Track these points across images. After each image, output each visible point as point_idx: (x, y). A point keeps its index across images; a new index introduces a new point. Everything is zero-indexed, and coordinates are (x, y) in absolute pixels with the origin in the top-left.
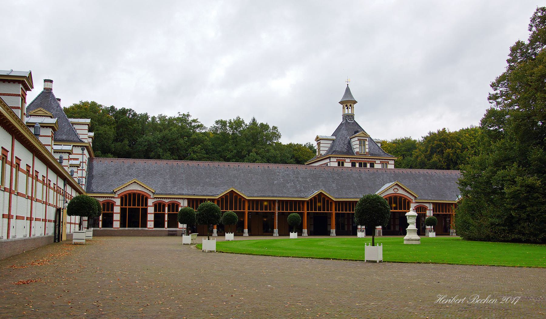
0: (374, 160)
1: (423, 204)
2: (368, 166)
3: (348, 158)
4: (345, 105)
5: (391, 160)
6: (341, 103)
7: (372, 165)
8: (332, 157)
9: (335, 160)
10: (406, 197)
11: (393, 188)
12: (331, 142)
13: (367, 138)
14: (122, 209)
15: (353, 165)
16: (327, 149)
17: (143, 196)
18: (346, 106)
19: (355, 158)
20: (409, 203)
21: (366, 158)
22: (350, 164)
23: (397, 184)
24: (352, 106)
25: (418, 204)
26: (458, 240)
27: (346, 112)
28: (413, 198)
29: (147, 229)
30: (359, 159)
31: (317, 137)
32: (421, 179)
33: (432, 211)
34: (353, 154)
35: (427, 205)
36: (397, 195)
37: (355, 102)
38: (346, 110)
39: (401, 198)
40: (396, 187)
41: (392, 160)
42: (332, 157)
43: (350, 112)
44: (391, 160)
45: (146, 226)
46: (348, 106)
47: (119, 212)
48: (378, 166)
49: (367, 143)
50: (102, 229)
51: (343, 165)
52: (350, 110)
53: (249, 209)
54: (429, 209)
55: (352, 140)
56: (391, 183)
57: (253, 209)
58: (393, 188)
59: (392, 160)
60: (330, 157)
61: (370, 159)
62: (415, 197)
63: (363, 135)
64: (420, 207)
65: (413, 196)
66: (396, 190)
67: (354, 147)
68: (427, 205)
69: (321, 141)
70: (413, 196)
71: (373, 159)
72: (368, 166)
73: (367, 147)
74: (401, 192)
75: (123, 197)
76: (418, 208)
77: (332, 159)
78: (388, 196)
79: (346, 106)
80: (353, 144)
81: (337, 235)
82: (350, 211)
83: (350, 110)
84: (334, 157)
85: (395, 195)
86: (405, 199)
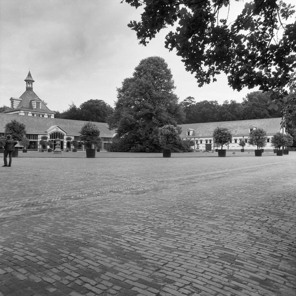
2: (41, 116)
6: (26, 81)
7: (43, 116)
9: (23, 111)
11: (56, 128)
12: (20, 102)
13: (41, 102)
15: (33, 115)
16: (17, 105)
18: (29, 83)
20: (63, 136)
22: (31, 114)
23: (58, 126)
26: (106, 152)
28: (65, 133)
31: (11, 98)
32: (69, 124)
34: (33, 109)
35: (72, 137)
37: (33, 81)
38: (28, 85)
39: (59, 133)
40: (57, 128)
46: (30, 82)
49: (40, 104)
55: (32, 102)
56: (55, 126)
58: (56, 128)
60: (20, 110)
62: (66, 133)
63: (38, 100)
65: (65, 132)
66: (57, 129)
67: (33, 105)
68: (72, 137)
69: (14, 101)
70: (65, 132)
72: (41, 116)
73: (40, 106)
74: (60, 130)
77: (21, 111)
78: (54, 132)
79: (29, 83)
80: (33, 104)
86: (62, 134)
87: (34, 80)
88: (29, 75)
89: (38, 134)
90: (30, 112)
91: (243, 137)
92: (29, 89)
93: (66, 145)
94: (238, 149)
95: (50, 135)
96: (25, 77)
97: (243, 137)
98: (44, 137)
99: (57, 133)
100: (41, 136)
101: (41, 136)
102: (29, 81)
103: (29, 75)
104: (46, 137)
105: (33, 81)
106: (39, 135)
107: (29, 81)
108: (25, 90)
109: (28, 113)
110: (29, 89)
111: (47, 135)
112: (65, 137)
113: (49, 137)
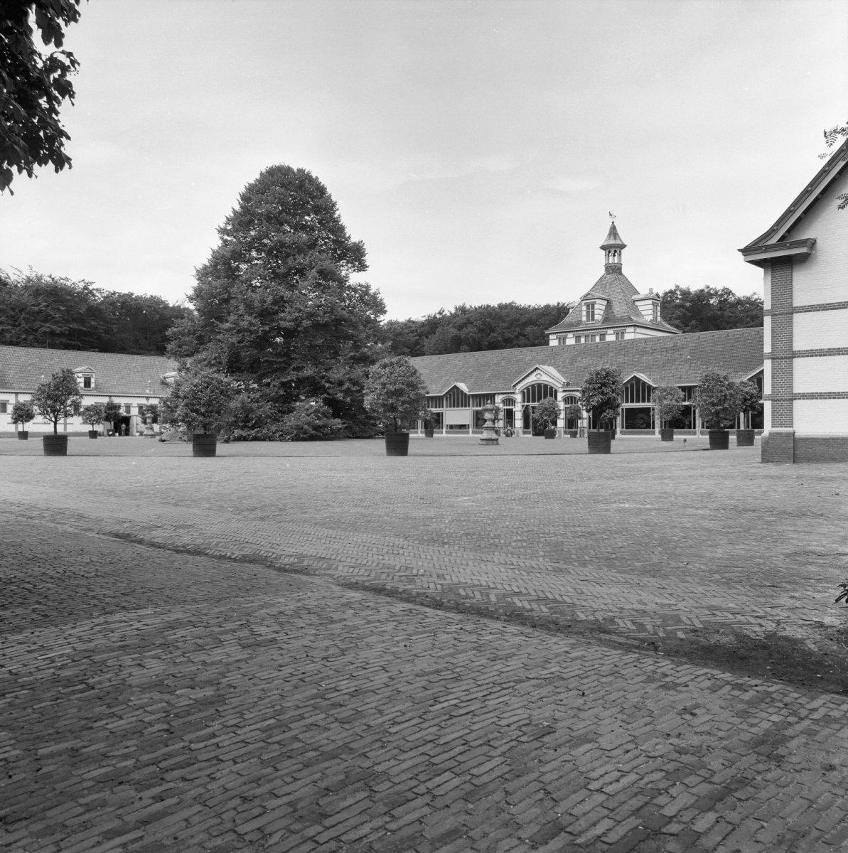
1: (573, 393)
5: (629, 326)
8: (551, 333)
11: (535, 373)
15: (578, 338)
20: (556, 391)
24: (618, 252)
25: (566, 393)
36: (539, 382)
39: (546, 386)
42: (551, 333)
44: (629, 326)
48: (611, 337)
52: (616, 258)
66: (538, 376)
84: (553, 333)
85: (537, 382)
87: (626, 244)
88: (613, 232)
89: (494, 395)
91: (17, 397)
92: (614, 270)
93: (520, 417)
94: (82, 431)
95: (523, 393)
96: (603, 239)
97: (17, 397)
98: (506, 400)
99: (539, 385)
102: (614, 248)
103: (613, 232)
104: (572, 397)
105: (623, 246)
106: (496, 397)
107: (614, 248)
108: (602, 271)
110: (614, 270)
111: (513, 393)
112: (560, 396)
113: (518, 397)
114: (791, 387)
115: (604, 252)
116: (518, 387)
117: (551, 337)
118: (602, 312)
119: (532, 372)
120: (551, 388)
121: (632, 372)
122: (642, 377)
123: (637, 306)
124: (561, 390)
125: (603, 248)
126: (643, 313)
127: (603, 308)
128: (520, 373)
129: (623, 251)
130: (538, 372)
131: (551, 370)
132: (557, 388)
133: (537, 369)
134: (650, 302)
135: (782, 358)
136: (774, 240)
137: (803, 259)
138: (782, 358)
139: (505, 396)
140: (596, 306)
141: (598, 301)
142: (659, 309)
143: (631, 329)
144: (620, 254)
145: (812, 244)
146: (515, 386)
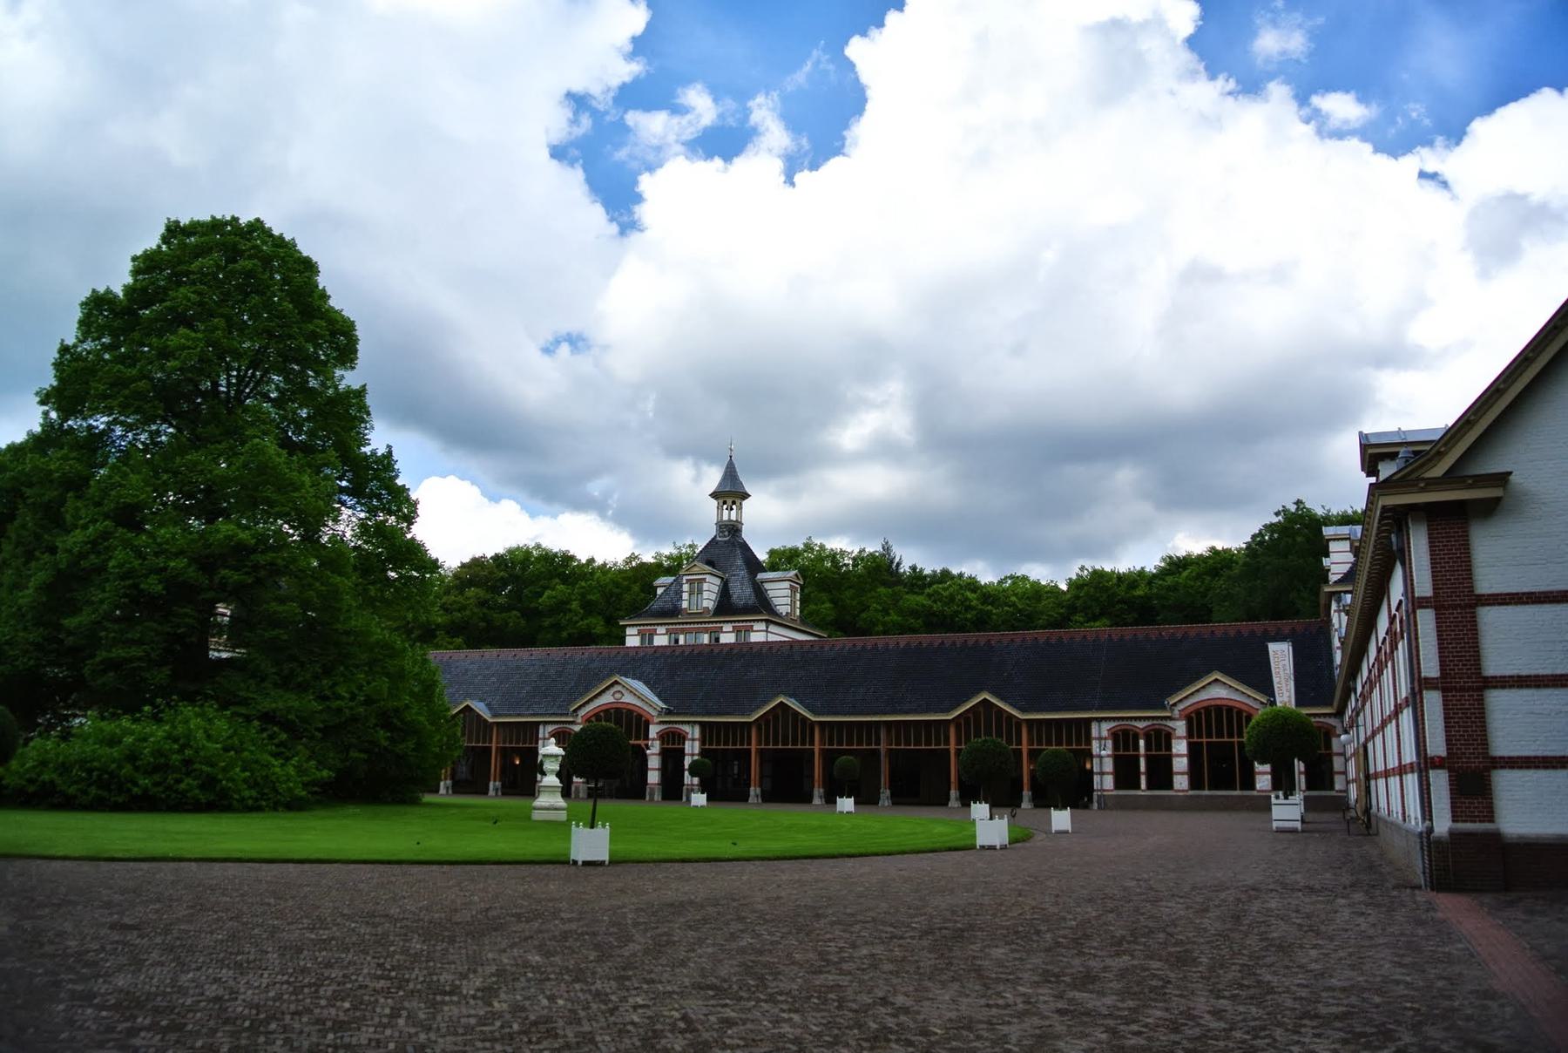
0: (718, 625)
1: (677, 726)
3: (661, 624)
4: (721, 501)
5: (758, 621)
8: (630, 625)
10: (640, 711)
14: (1190, 745)
17: (1240, 712)
19: (679, 623)
20: (647, 723)
21: (701, 623)
27: (725, 518)
29: (1255, 793)
30: (685, 626)
33: (697, 744)
35: (687, 728)
38: (726, 512)
39: (630, 712)
41: (762, 620)
43: (733, 517)
45: (1252, 786)
47: (1186, 752)
50: (1149, 793)
51: (651, 640)
52: (733, 513)
53: (759, 743)
54: (690, 736)
57: (711, 744)
59: (762, 620)
61: (709, 622)
64: (564, 732)
66: (618, 696)
68: (687, 728)
71: (716, 622)
75: (1192, 718)
76: (667, 734)
81: (894, 803)
82: (726, 743)
83: (733, 513)
84: (633, 625)
85: (615, 706)
89: (538, 723)
90: (660, 630)
99: (617, 709)
100: (550, 728)
101: (550, 728)
105: (745, 496)
106: (541, 728)
109: (652, 634)
114: (1485, 743)
115: (714, 503)
116: (582, 713)
117: (629, 631)
118: (714, 597)
119: (607, 688)
120: (640, 716)
121: (776, 695)
122: (792, 703)
123: (766, 591)
124: (656, 720)
125: (715, 495)
126: (776, 601)
127: (716, 589)
128: (587, 690)
129: (745, 503)
130: (617, 688)
131: (639, 686)
132: (648, 716)
133: (616, 683)
134: (787, 584)
135: (1462, 689)
136: (1438, 471)
137: (1488, 509)
138: (1462, 689)
139: (556, 726)
140: (705, 586)
141: (708, 578)
142: (798, 596)
143: (762, 626)
144: (740, 508)
145: (1502, 479)
146: (575, 711)
